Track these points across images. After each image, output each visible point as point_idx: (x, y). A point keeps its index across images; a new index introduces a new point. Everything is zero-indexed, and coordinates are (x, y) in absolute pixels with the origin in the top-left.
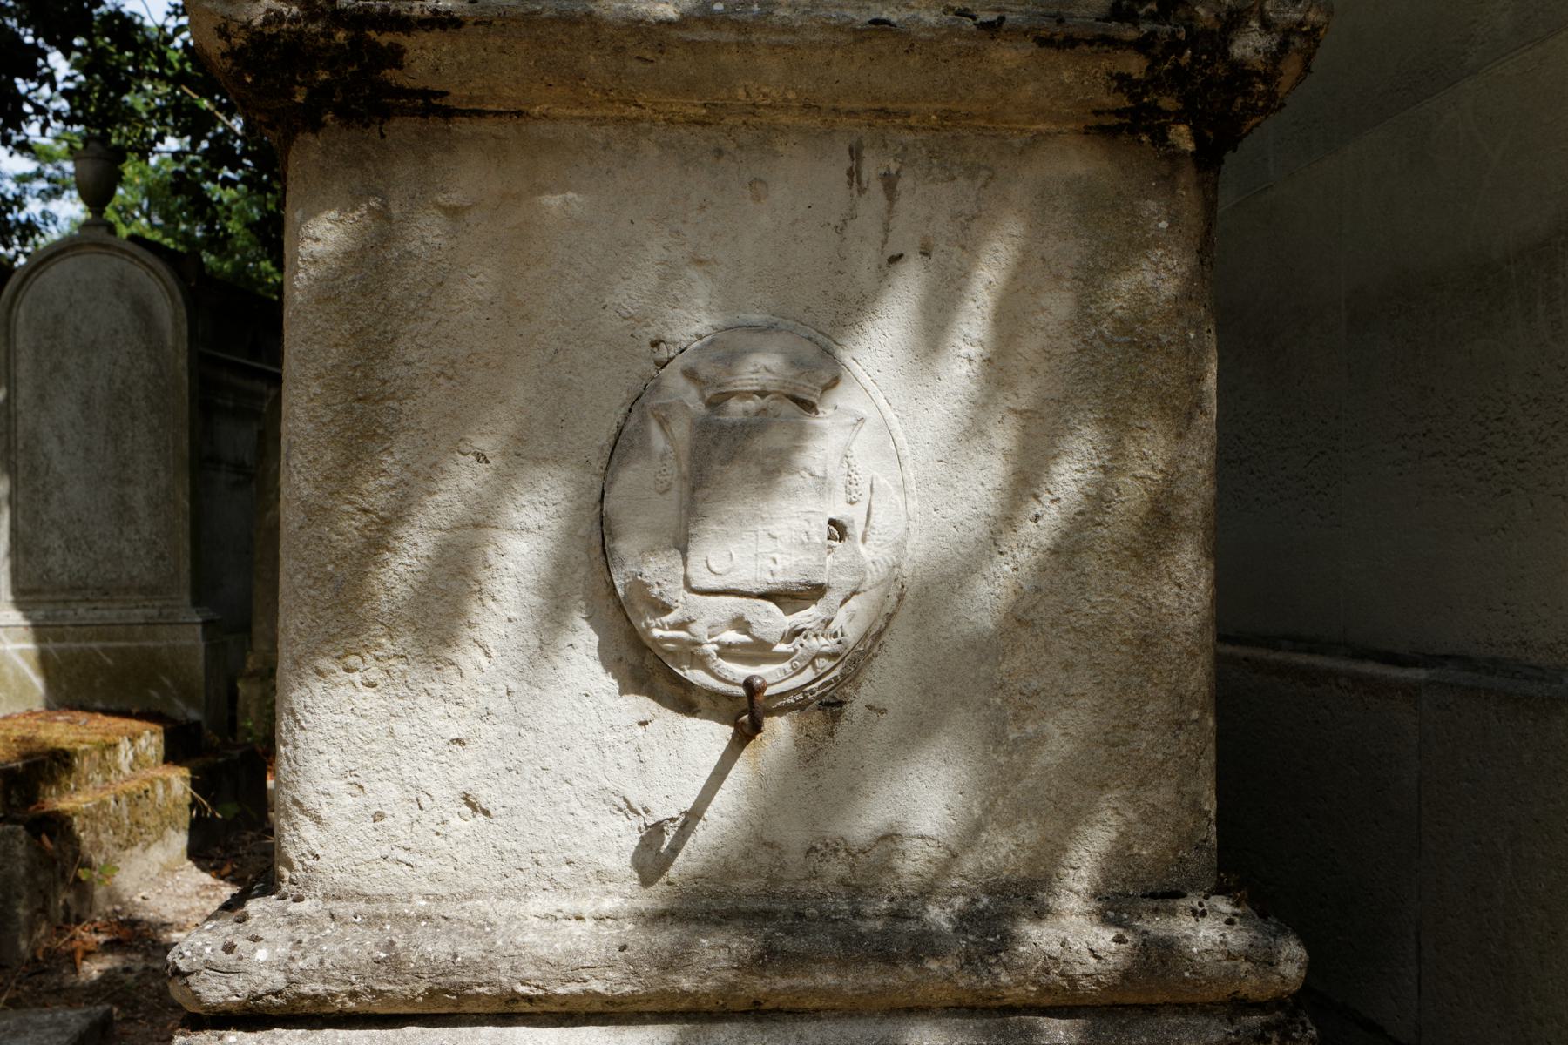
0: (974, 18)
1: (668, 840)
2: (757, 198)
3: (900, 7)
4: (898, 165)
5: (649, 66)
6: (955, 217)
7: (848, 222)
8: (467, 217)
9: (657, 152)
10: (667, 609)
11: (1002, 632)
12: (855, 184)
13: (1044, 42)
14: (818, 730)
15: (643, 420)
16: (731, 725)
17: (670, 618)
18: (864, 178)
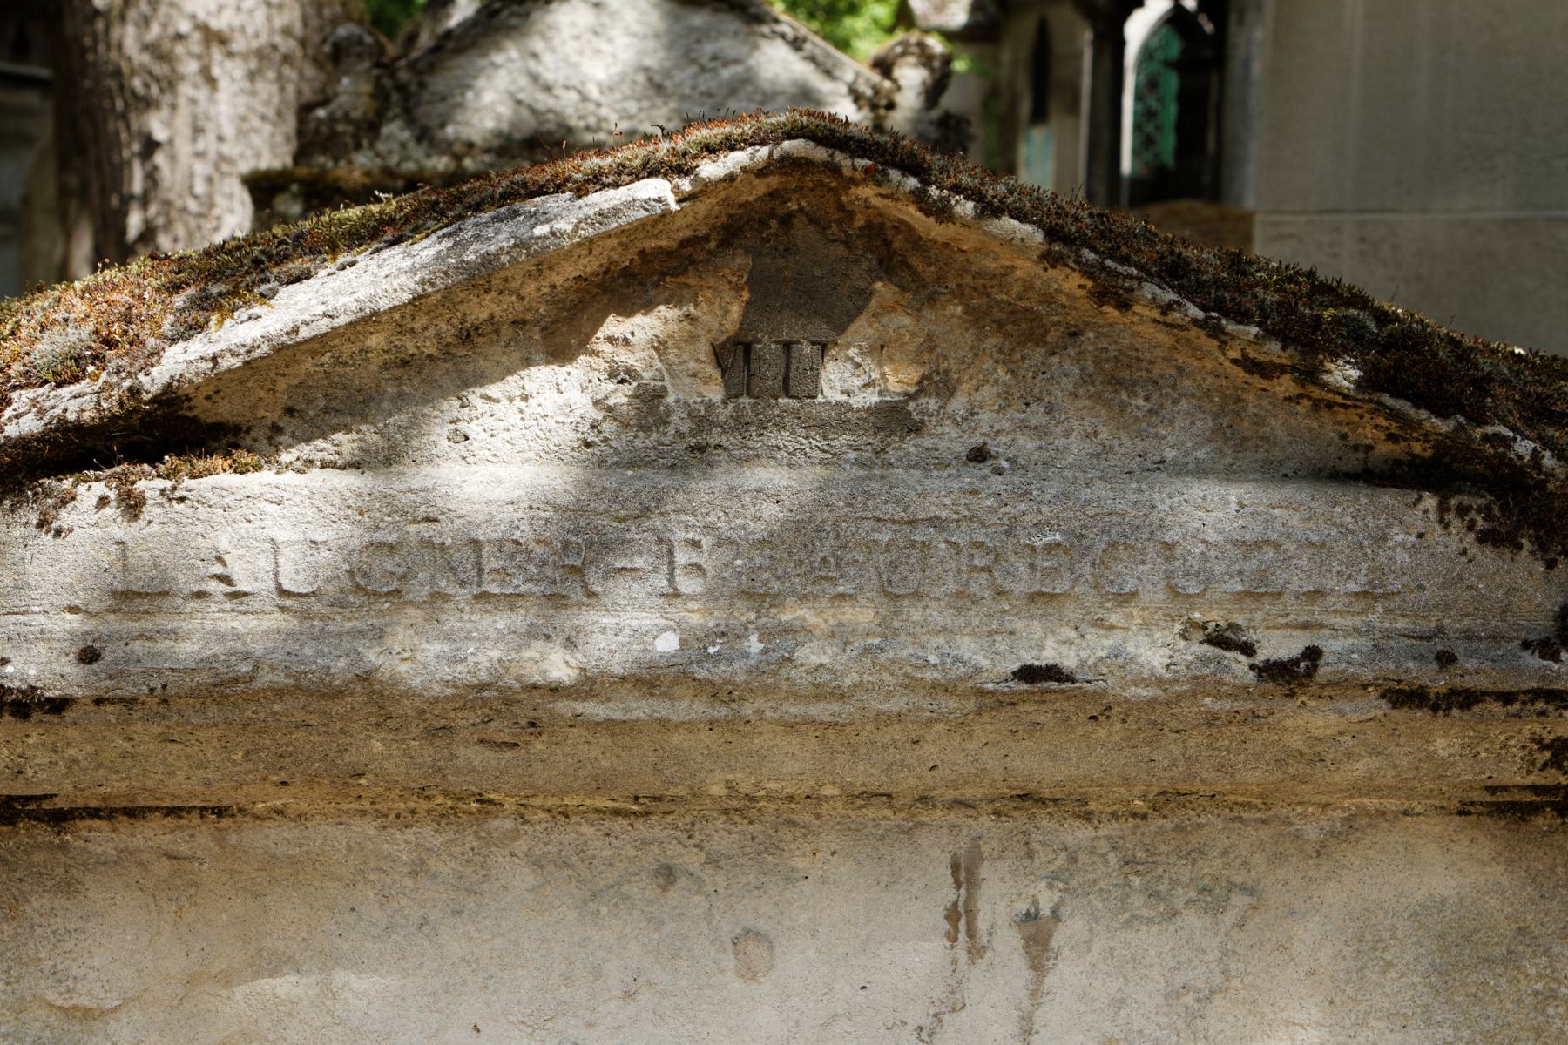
0: (1248, 649)
2: (750, 973)
3: (1083, 627)
4: (1056, 896)
5: (509, 754)
6: (1174, 994)
7: (946, 1018)
8: (113, 1025)
9: (531, 879)
12: (962, 936)
13: (1406, 697)
18: (982, 925)
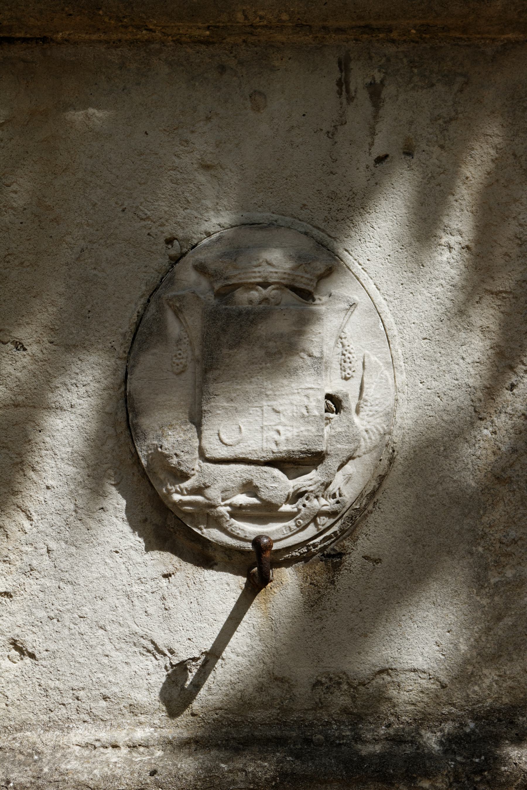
1: (191, 677)
2: (257, 109)
4: (382, 75)
7: (339, 127)
10: (185, 477)
11: (485, 490)
12: (344, 93)
14: (322, 579)
15: (160, 310)
16: (244, 576)
17: (187, 484)
18: (352, 88)
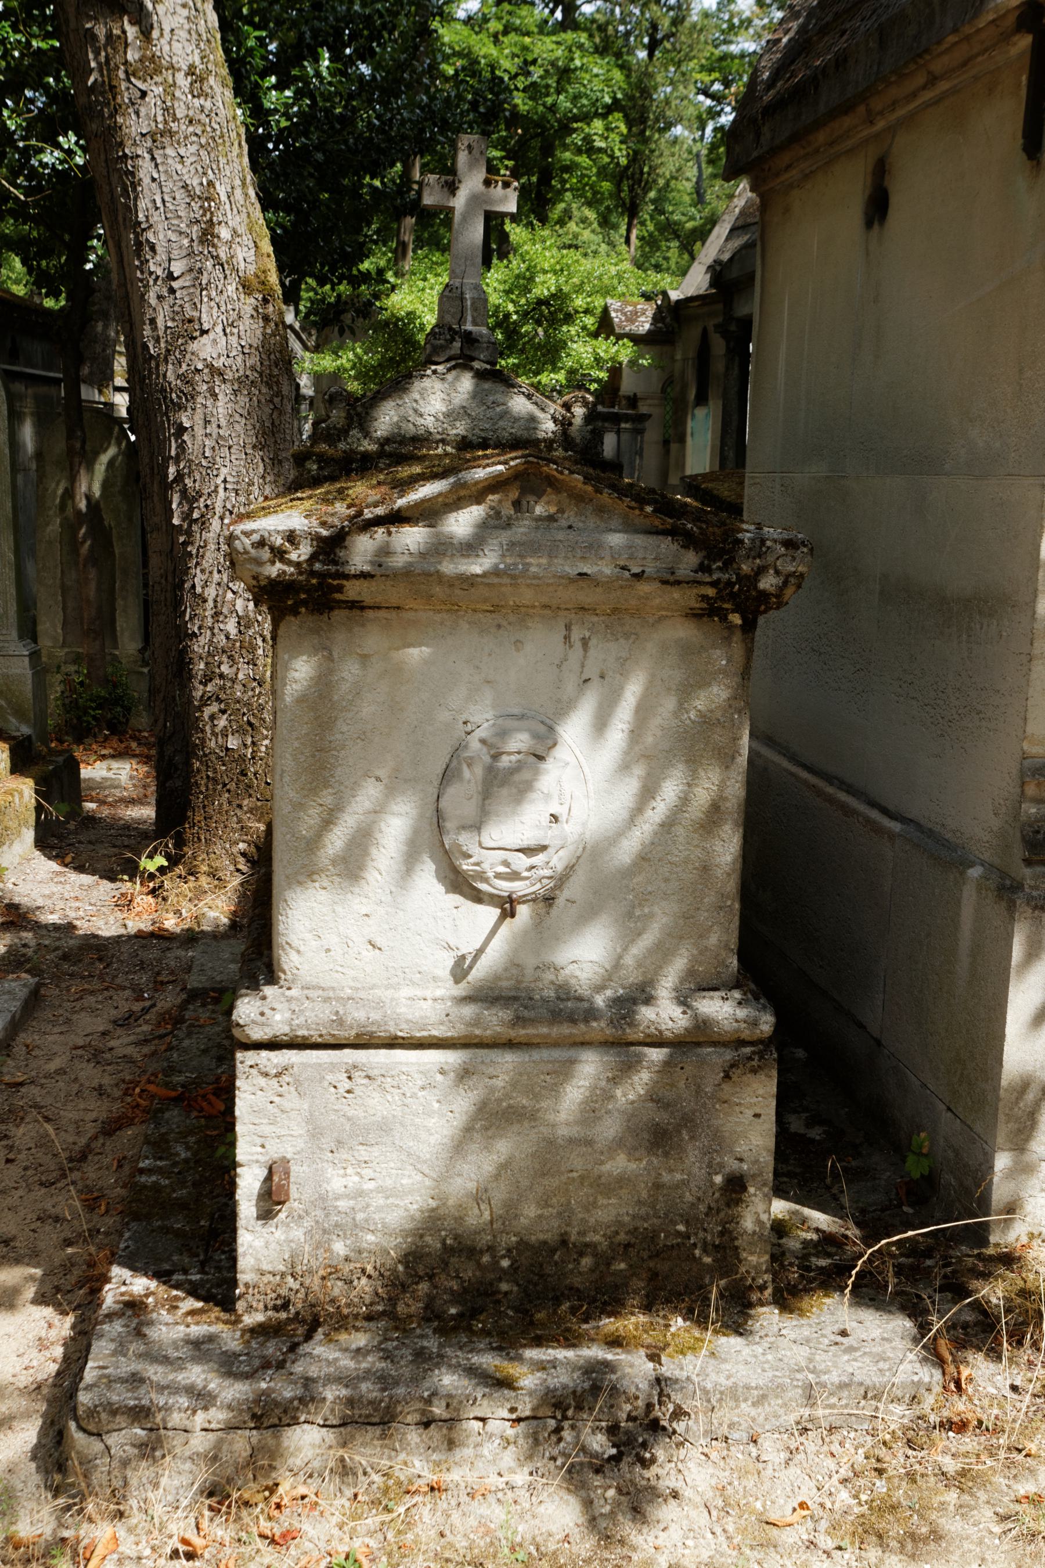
1: (468, 962)
2: (518, 650)
6: (618, 659)
10: (470, 856)
11: (635, 864)
13: (665, 582)
14: (543, 911)
15: (459, 763)
17: (471, 860)
